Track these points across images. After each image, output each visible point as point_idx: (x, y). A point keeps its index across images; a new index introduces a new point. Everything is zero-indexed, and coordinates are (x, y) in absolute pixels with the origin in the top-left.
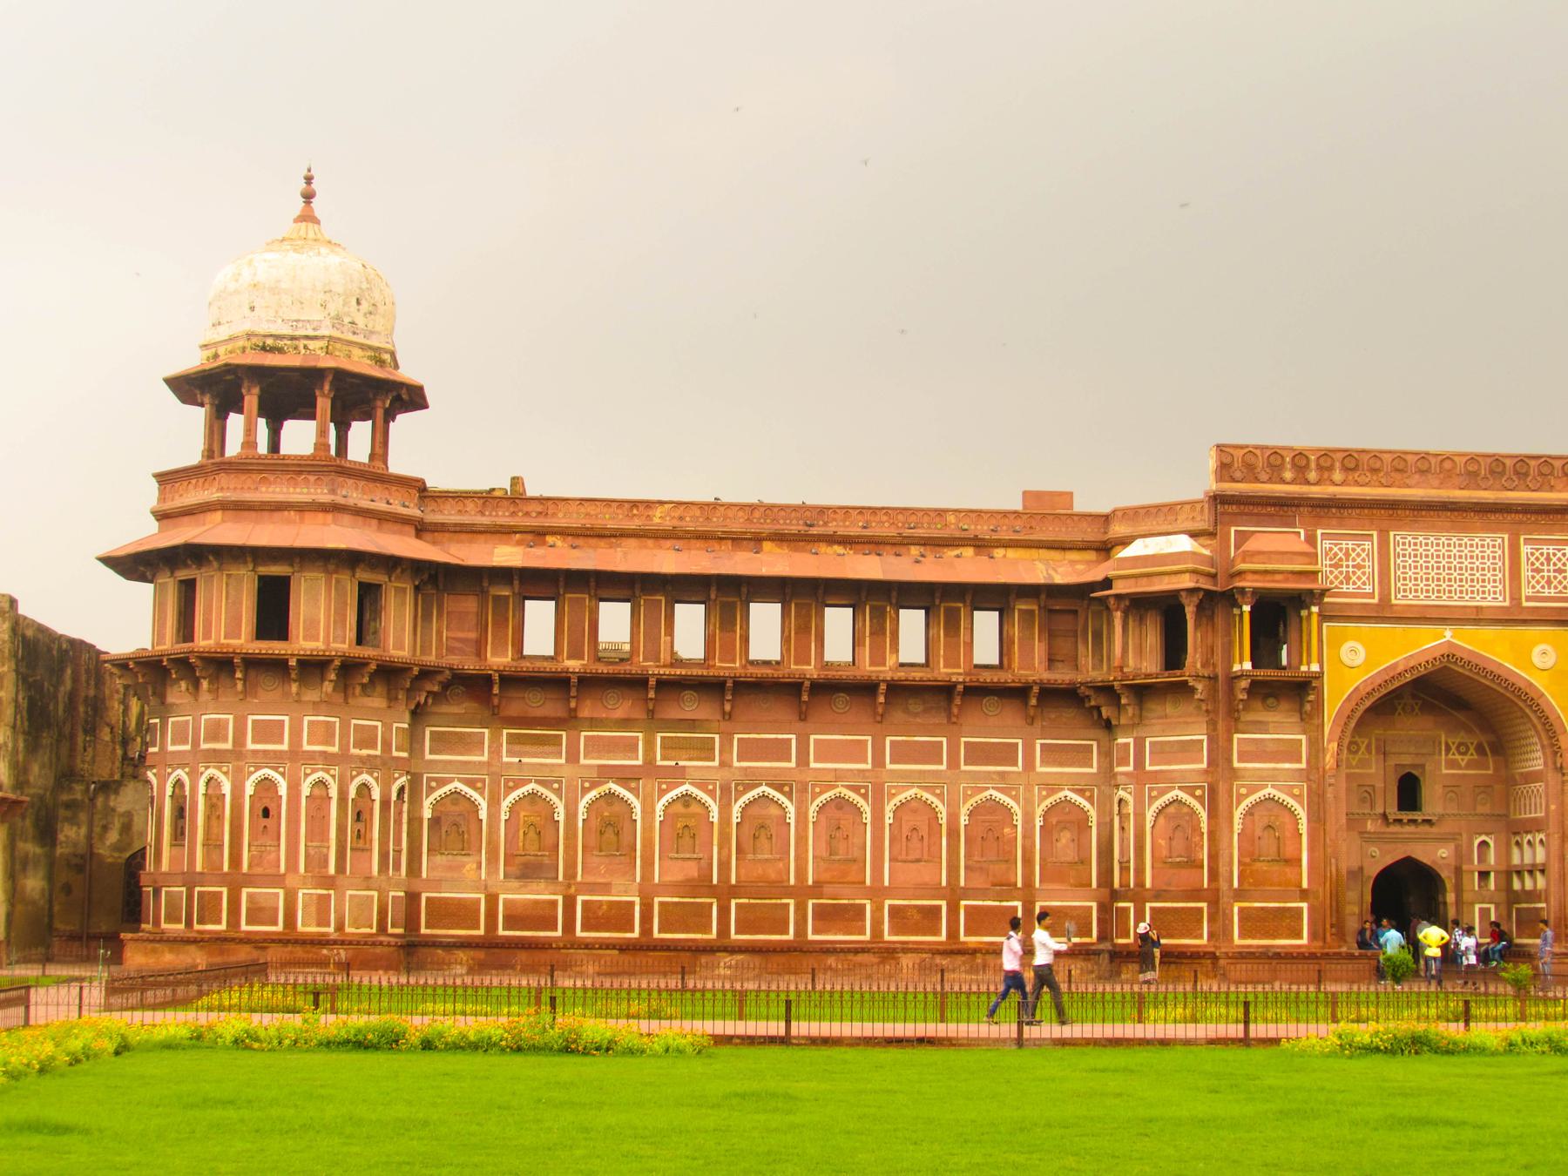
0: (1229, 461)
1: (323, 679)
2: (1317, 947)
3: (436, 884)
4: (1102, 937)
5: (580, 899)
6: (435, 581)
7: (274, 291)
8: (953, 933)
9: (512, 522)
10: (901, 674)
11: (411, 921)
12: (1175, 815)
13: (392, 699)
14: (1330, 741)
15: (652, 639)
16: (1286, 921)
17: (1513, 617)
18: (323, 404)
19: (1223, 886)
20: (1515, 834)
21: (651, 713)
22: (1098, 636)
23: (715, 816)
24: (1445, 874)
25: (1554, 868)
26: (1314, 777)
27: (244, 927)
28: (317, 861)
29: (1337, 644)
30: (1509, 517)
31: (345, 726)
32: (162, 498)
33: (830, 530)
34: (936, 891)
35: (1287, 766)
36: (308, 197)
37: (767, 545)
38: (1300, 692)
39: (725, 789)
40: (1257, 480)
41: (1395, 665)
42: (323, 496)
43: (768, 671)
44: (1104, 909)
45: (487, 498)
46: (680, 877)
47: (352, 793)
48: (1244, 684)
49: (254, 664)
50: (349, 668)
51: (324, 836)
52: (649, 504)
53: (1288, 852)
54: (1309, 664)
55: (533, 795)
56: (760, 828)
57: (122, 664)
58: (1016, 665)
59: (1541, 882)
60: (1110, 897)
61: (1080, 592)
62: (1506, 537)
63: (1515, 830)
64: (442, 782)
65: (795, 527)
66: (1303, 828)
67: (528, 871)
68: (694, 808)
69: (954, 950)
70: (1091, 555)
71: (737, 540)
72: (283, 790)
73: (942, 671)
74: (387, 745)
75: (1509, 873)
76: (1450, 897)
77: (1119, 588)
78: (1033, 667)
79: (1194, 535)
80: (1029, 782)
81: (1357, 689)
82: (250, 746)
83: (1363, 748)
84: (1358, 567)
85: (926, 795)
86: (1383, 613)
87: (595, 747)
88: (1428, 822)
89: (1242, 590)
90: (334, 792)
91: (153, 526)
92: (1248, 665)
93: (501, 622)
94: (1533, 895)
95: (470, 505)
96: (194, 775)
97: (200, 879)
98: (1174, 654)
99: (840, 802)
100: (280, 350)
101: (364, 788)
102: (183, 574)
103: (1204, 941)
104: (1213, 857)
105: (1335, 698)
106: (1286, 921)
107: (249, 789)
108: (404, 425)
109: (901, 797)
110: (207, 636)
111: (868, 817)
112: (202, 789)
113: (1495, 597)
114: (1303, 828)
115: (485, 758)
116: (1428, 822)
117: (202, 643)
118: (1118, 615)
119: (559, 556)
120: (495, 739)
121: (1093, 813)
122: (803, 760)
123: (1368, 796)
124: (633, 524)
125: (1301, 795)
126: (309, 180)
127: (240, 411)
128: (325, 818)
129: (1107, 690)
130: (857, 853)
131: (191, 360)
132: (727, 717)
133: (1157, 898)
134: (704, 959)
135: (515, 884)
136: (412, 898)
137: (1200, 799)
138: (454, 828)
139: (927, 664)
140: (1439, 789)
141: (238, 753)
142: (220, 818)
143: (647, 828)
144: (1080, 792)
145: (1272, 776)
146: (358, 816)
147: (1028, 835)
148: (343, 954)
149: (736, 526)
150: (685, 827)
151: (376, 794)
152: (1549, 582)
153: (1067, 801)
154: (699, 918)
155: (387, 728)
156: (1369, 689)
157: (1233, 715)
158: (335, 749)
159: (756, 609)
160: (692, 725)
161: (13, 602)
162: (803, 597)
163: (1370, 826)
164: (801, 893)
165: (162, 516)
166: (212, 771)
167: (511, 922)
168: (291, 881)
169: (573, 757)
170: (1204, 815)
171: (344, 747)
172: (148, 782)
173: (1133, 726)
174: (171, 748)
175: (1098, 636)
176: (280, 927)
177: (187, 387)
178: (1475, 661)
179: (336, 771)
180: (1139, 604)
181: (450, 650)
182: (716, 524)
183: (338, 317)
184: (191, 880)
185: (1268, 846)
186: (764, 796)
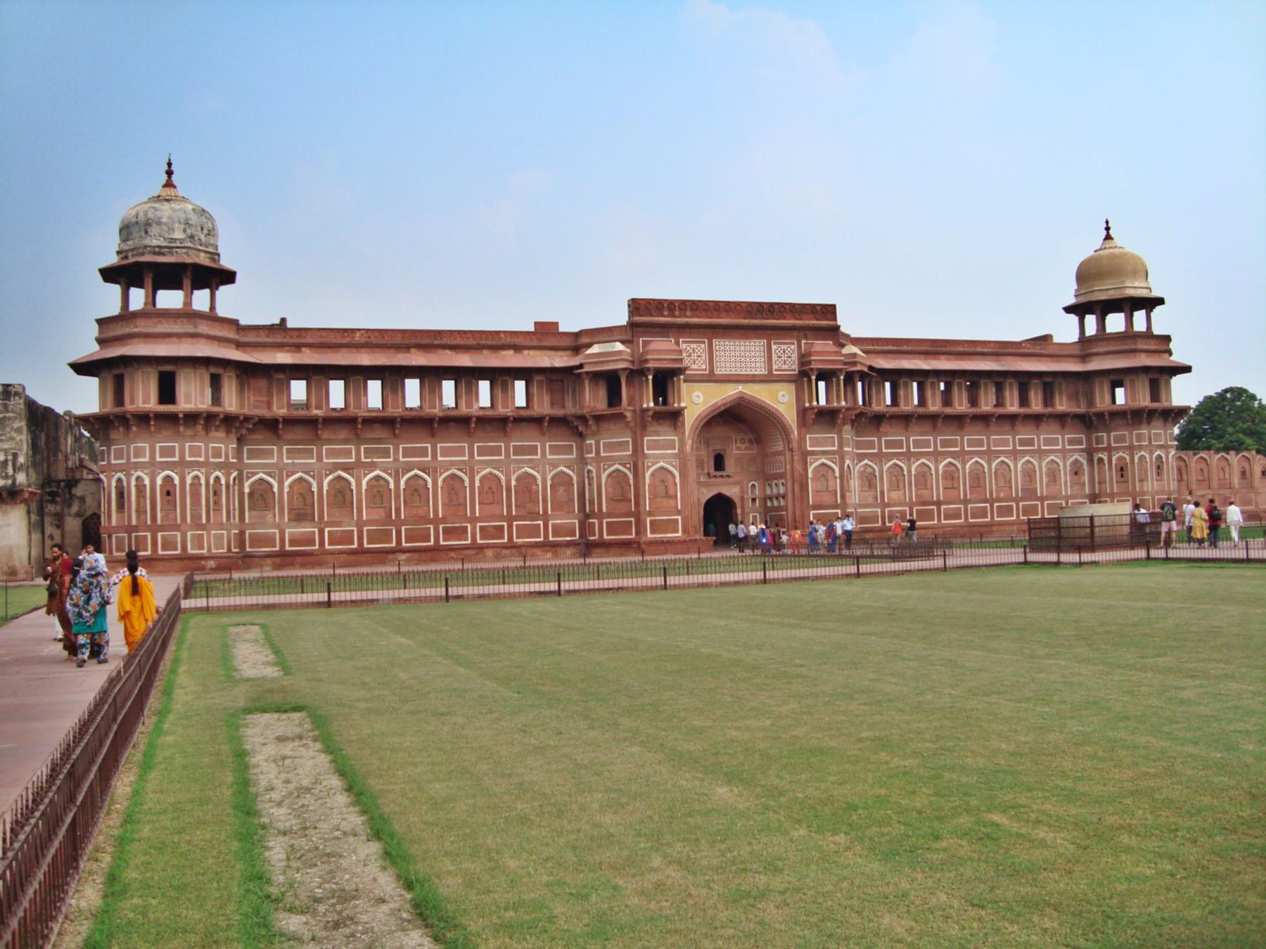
0: (636, 306)
1: (195, 423)
2: (686, 538)
3: (252, 526)
4: (581, 537)
5: (327, 530)
6: (247, 371)
7: (159, 223)
8: (510, 538)
9: (285, 341)
10: (481, 413)
11: (242, 545)
12: (618, 477)
13: (228, 432)
15: (357, 398)
16: (672, 525)
17: (769, 379)
18: (187, 283)
19: (642, 509)
21: (357, 436)
22: (574, 392)
23: (392, 486)
24: (737, 501)
25: (790, 495)
26: (681, 456)
27: (160, 552)
28: (196, 517)
29: (690, 393)
30: (768, 332)
31: (207, 448)
32: (101, 331)
33: (444, 341)
34: (502, 518)
36: (170, 173)
37: (413, 350)
38: (675, 417)
39: (397, 473)
40: (651, 315)
42: (188, 328)
43: (374, 414)
44: (580, 523)
45: (271, 329)
46: (376, 517)
47: (212, 481)
48: (650, 413)
49: (160, 417)
51: (200, 505)
52: (353, 331)
54: (679, 402)
55: (301, 479)
56: (416, 490)
57: (85, 420)
58: (536, 407)
59: (782, 503)
60: (585, 517)
61: (568, 371)
63: (767, 479)
64: (254, 474)
65: (426, 341)
66: (678, 481)
67: (301, 515)
68: (382, 482)
69: (511, 546)
70: (569, 353)
71: (399, 348)
72: (177, 481)
73: (502, 410)
74: (227, 457)
75: (766, 498)
76: (739, 511)
77: (586, 369)
78: (544, 407)
79: (622, 342)
80: (545, 461)
82: (158, 459)
85: (495, 472)
86: (711, 378)
87: (331, 454)
88: (728, 476)
89: (648, 369)
90: (203, 481)
91: (96, 347)
92: (652, 404)
93: (280, 392)
94: (779, 509)
95: (262, 333)
96: (128, 476)
97: (136, 529)
98: (614, 397)
99: (453, 476)
100: (163, 254)
101: (217, 479)
102: (116, 372)
103: (633, 536)
104: (637, 496)
105: (690, 418)
106: (672, 525)
107: (159, 481)
108: (224, 291)
109: (484, 473)
110: (132, 402)
111: (467, 483)
112: (133, 482)
113: (761, 370)
114: (678, 481)
115: (275, 461)
116: (728, 476)
117: (129, 407)
118: (587, 382)
119: (308, 357)
120: (280, 451)
121: (575, 478)
122: (434, 456)
123: (700, 465)
124: (346, 341)
126: (170, 164)
127: (141, 286)
128: (199, 495)
129: (583, 418)
130: (461, 501)
131: (112, 259)
132: (395, 435)
133: (609, 515)
134: (391, 557)
135: (294, 524)
136: (242, 533)
137: (629, 469)
138: (261, 496)
139: (528, 406)
140: (732, 461)
141: (153, 463)
142: (145, 497)
143: (359, 492)
144: (568, 467)
145: (663, 457)
146: (215, 493)
147: (544, 489)
148: (212, 564)
149: (398, 340)
150: (378, 491)
151: (223, 481)
153: (562, 472)
154: (386, 536)
155: (227, 447)
157: (644, 427)
158: (202, 459)
159: (407, 381)
160: (379, 441)
161: (24, 388)
162: (430, 376)
163: (702, 479)
164: (436, 521)
165: (100, 341)
166: (139, 473)
167: (292, 543)
168: (183, 528)
169: (320, 459)
170: (631, 476)
171: (207, 458)
172: (99, 480)
173: (594, 434)
174: (113, 462)
175: (574, 392)
176: (179, 552)
177: (109, 274)
179: (203, 470)
180: (596, 376)
181: (255, 407)
182: (387, 340)
183: (192, 237)
184: (130, 529)
185: (661, 490)
186: (416, 475)
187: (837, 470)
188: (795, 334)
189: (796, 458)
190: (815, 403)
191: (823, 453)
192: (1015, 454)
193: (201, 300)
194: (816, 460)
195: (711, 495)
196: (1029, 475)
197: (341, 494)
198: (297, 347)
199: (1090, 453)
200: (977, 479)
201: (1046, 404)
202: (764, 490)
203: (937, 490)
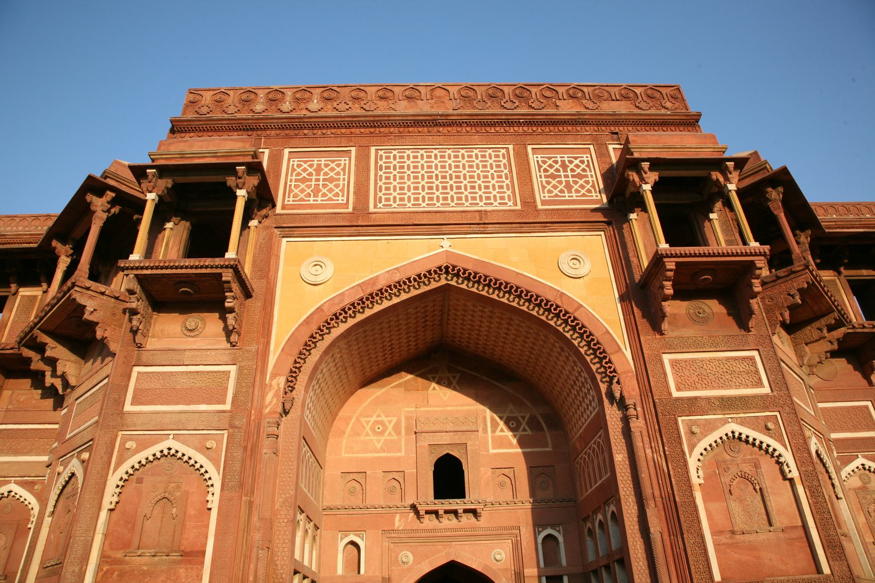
14: (274, 375)
17: (527, 221)
20: (585, 520)
35: (203, 407)
41: (374, 280)
53: (188, 540)
62: (511, 147)
66: (214, 502)
81: (320, 309)
83: (390, 427)
84: (331, 180)
86: (359, 223)
88: (474, 512)
125: (219, 449)
140: (486, 472)
144: (28, 485)
145: (177, 425)
152: (569, 187)
156: (337, 309)
163: (398, 523)
178: (482, 271)
187: (788, 457)
188: (589, 130)
189: (637, 425)
190: (664, 246)
191: (727, 404)
194: (710, 427)
195: (426, 568)
202: (583, 552)
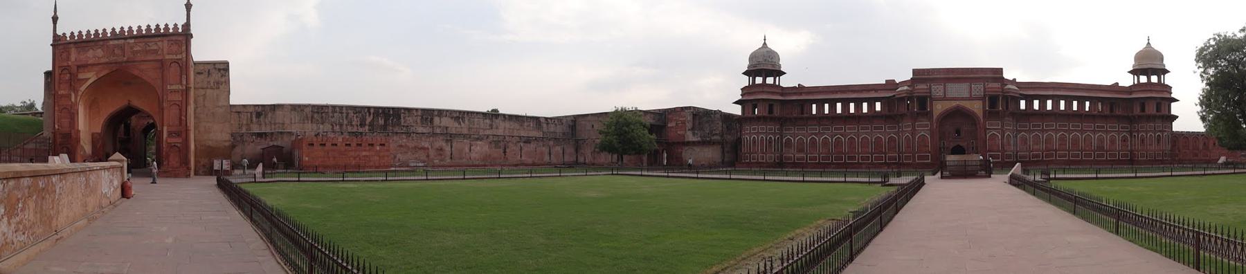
0: (915, 72)
17: (970, 99)
38: (929, 115)
50: (764, 118)
56: (838, 142)
67: (801, 150)
69: (872, 164)
80: (884, 134)
86: (945, 99)
150: (825, 142)
180: (902, 99)
192: (1094, 132)
193: (770, 80)
196: (1101, 140)
197: (813, 142)
198: (801, 94)
199: (1131, 133)
200: (1075, 142)
201: (1111, 110)
203: (1056, 145)
